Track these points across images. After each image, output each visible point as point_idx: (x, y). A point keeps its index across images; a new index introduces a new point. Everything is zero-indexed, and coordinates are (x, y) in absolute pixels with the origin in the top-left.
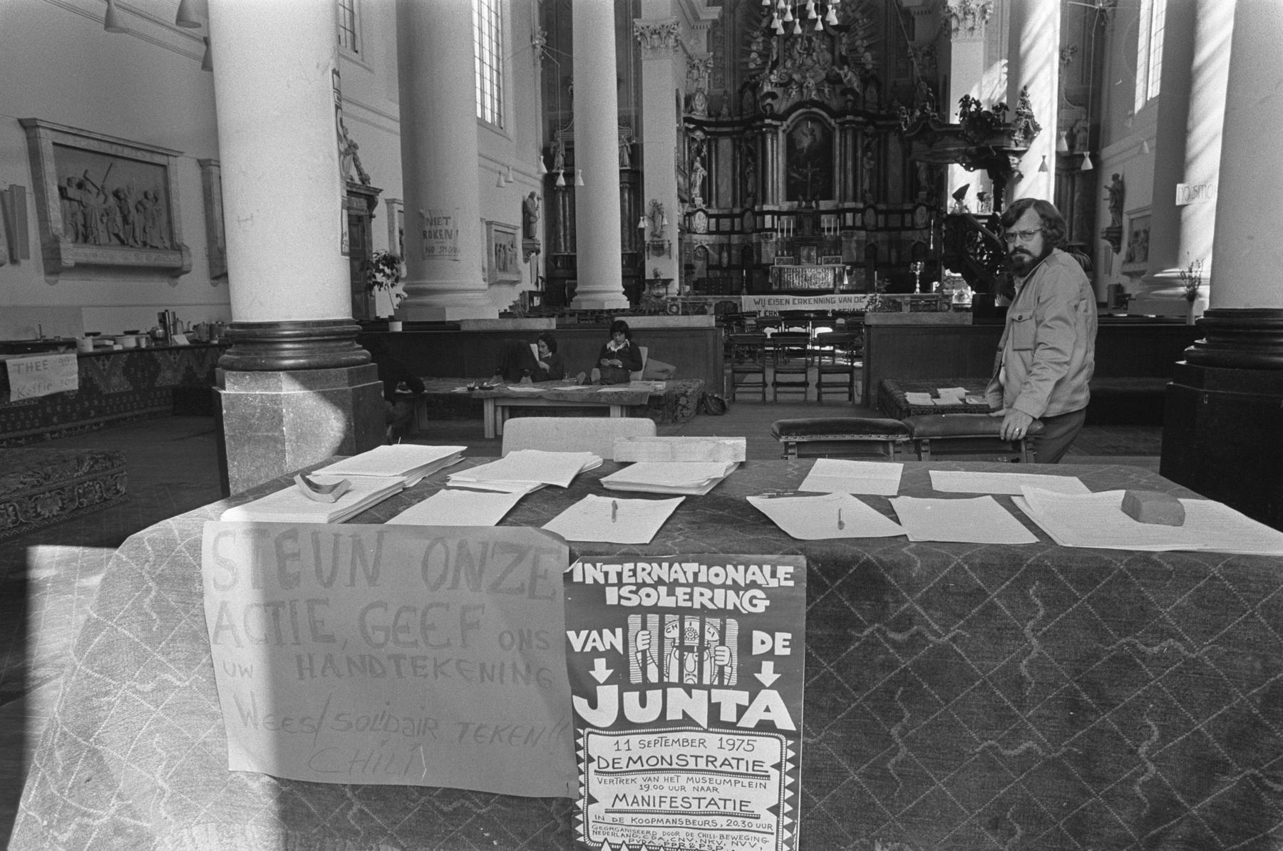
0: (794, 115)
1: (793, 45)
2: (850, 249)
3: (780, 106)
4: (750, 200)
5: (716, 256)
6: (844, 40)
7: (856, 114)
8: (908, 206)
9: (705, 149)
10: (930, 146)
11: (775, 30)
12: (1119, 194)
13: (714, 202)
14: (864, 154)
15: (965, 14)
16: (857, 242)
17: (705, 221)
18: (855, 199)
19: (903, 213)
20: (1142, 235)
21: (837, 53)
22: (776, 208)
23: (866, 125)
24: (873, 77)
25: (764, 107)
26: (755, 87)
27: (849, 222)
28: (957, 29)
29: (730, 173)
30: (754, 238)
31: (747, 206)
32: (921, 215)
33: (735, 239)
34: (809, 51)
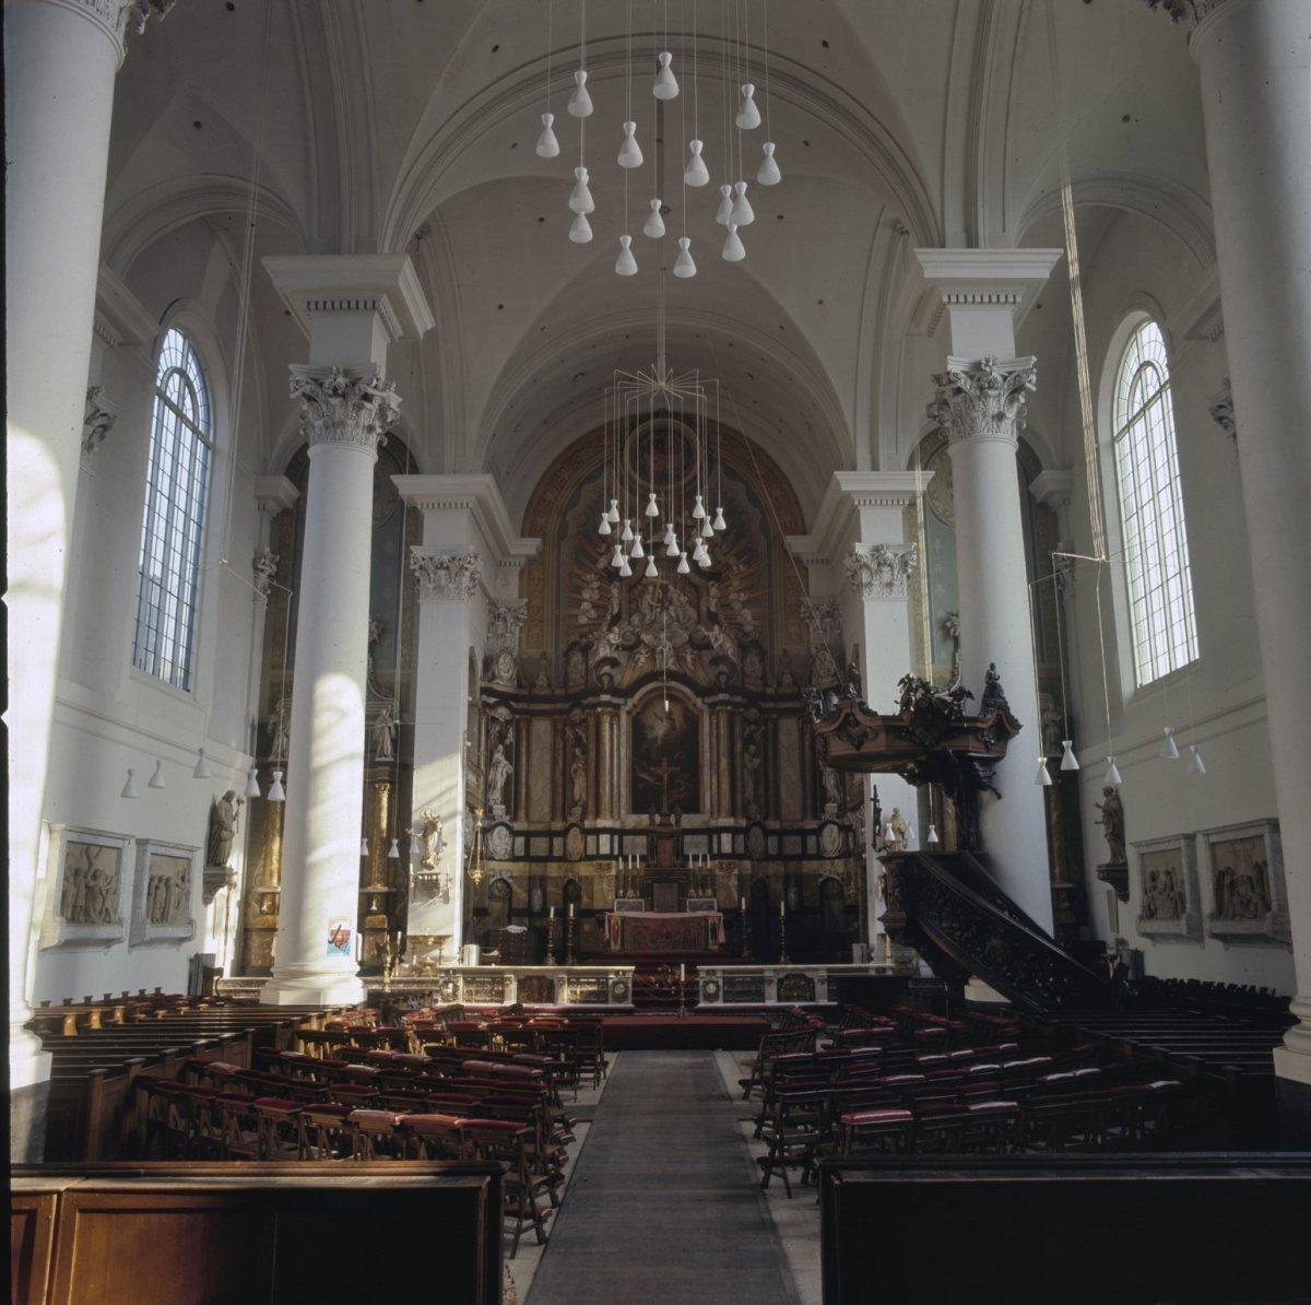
0: (644, 690)
1: (643, 593)
3: (624, 677)
4: (578, 810)
5: (524, 896)
6: (713, 591)
7: (732, 691)
8: (812, 824)
9: (511, 735)
10: (858, 748)
11: (618, 569)
12: (1115, 819)
13: (522, 813)
14: (745, 749)
15: (879, 564)
16: (740, 877)
17: (508, 840)
18: (733, 814)
19: (803, 833)
20: (1163, 877)
21: (704, 609)
22: (617, 825)
23: (746, 707)
24: (755, 643)
25: (600, 678)
26: (586, 650)
27: (727, 847)
28: (870, 584)
29: (548, 773)
30: (585, 869)
31: (571, 820)
32: (831, 838)
33: (553, 870)
34: (664, 602)
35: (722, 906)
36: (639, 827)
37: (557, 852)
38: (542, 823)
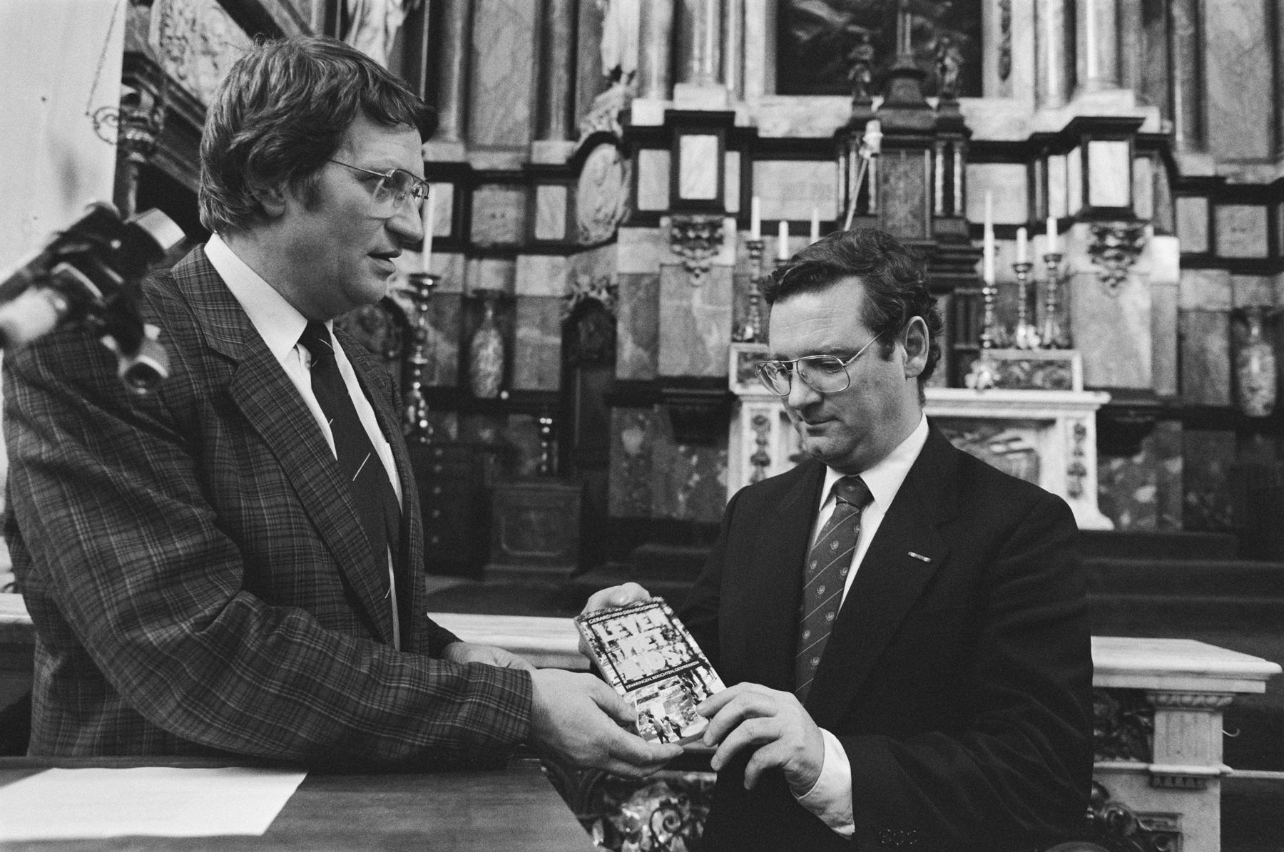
2: (1115, 318)
5: (445, 350)
13: (451, 119)
35: (1097, 381)
36: (805, 133)
37: (550, 225)
38: (505, 149)
